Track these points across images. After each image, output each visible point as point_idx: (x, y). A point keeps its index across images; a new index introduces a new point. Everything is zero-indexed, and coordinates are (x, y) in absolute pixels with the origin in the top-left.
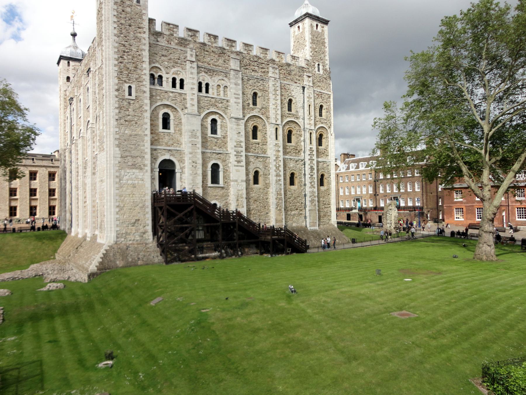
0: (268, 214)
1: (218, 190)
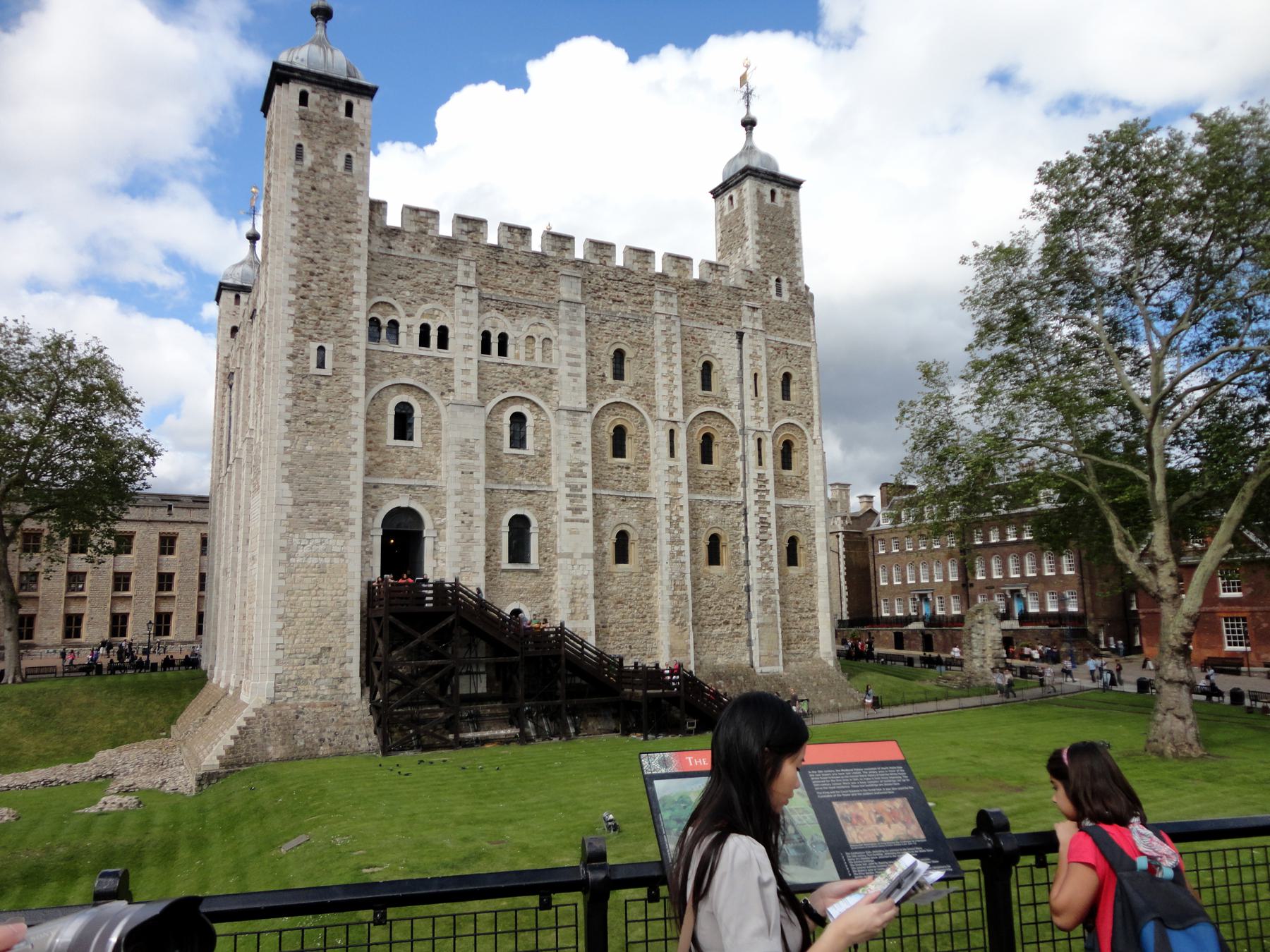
0: (652, 636)
1: (525, 578)
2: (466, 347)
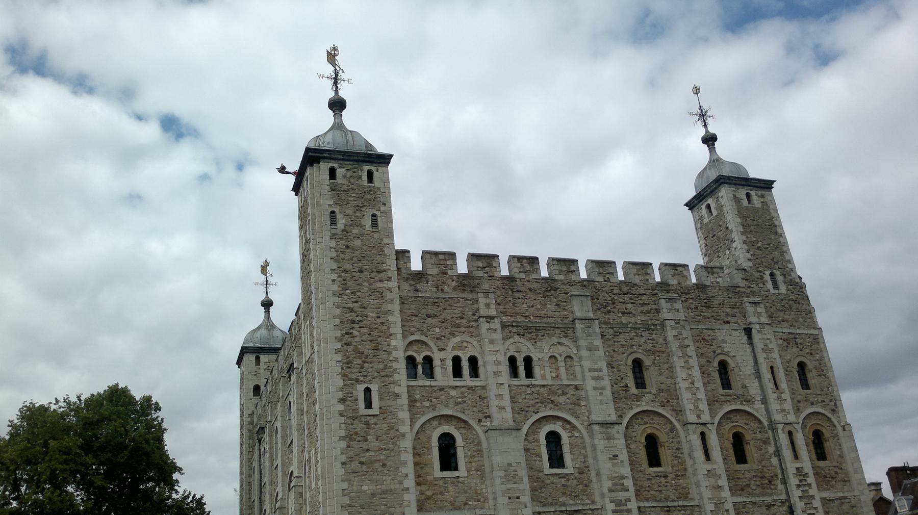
2: (496, 374)
